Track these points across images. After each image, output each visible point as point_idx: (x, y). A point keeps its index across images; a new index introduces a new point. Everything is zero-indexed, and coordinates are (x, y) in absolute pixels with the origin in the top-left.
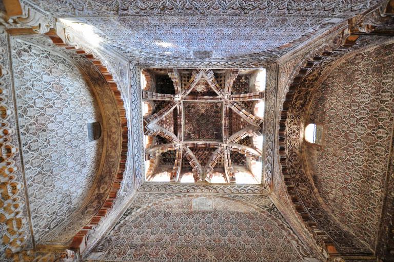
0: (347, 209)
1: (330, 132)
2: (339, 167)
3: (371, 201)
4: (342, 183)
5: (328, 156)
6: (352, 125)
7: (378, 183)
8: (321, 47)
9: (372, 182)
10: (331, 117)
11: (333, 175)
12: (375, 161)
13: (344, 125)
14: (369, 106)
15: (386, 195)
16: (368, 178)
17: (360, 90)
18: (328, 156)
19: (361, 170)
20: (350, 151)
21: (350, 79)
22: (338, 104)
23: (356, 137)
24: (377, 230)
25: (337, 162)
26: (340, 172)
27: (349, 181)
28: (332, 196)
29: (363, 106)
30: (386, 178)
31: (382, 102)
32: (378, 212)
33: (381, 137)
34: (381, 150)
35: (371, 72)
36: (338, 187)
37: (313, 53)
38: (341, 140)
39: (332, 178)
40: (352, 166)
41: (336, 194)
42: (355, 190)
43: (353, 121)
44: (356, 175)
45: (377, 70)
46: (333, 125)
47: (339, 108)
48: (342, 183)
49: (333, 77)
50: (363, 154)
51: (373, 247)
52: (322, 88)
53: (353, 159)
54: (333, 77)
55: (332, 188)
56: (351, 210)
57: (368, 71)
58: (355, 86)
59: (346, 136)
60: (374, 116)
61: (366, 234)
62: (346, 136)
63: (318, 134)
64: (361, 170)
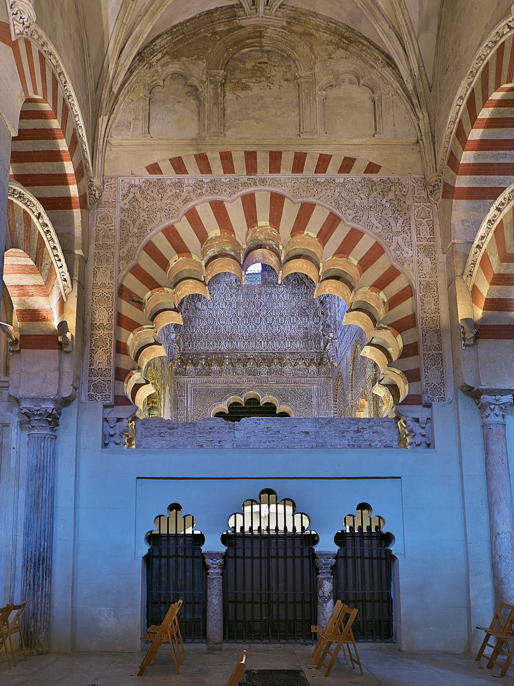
0: (197, 323)
1: (257, 296)
5: (234, 296)
6: (266, 318)
8: (328, 311)
10: (270, 294)
11: (219, 304)
13: (265, 311)
14: (282, 332)
15: (225, 353)
16: (231, 338)
17: (294, 323)
18: (234, 296)
19: (234, 332)
20: (246, 321)
21: (303, 313)
22: (282, 302)
23: (258, 324)
26: (225, 312)
29: (282, 327)
31: (284, 342)
32: (211, 350)
33: (261, 344)
34: (252, 345)
35: (306, 331)
37: (326, 301)
38: (253, 310)
42: (217, 329)
43: (269, 320)
45: (306, 336)
46: (264, 299)
47: (279, 304)
49: (307, 293)
50: (246, 332)
52: (298, 281)
53: (240, 324)
54: (307, 293)
56: (199, 327)
57: (306, 328)
58: (297, 319)
59: (257, 315)
60: (275, 337)
61: (189, 342)
62: (257, 315)
64: (234, 332)
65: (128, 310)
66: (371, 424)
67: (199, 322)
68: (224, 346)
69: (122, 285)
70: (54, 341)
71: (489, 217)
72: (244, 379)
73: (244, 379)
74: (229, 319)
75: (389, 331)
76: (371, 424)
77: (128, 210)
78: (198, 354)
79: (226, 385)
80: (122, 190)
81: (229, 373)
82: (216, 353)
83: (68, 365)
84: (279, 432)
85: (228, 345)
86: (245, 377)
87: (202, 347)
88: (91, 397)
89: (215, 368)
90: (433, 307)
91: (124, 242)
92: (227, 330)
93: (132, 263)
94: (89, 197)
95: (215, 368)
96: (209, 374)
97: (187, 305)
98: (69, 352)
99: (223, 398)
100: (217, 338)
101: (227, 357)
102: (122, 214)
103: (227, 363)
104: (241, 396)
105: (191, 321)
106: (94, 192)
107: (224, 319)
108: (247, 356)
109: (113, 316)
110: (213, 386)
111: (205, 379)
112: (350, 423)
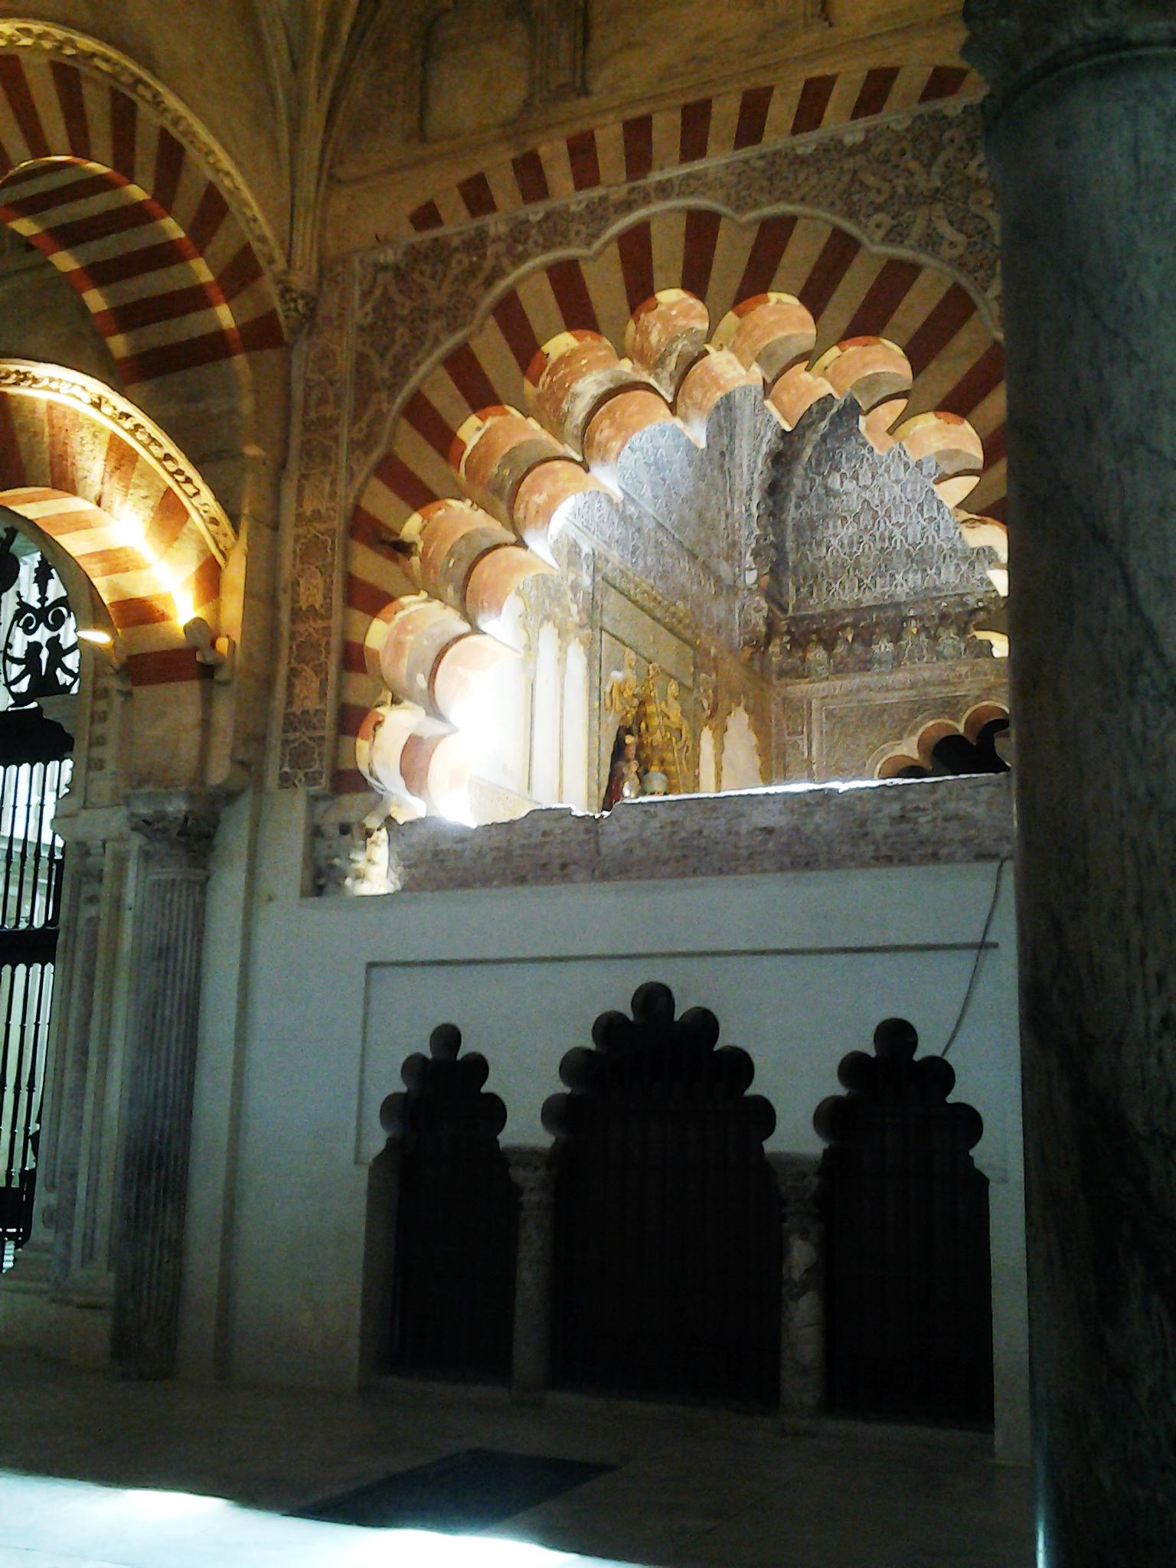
0: (831, 531)
2: (915, 482)
3: (878, 580)
4: (882, 502)
7: (919, 582)
9: (916, 572)
11: (887, 470)
12: (957, 565)
15: (905, 603)
24: (832, 606)
25: (925, 472)
27: (894, 521)
28: (834, 481)
30: (935, 594)
36: (867, 495)
39: (881, 471)
40: (932, 519)
41: (846, 493)
44: (914, 532)
48: (882, 502)
51: (797, 608)
53: (947, 516)
56: (835, 542)
61: (811, 586)
65: (369, 565)
66: (937, 796)
67: (835, 527)
68: (904, 584)
69: (357, 508)
70: (190, 663)
72: (963, 670)
73: (963, 670)
74: (914, 508)
76: (937, 796)
77: (372, 327)
78: (833, 615)
79: (913, 692)
80: (361, 283)
81: (921, 658)
82: (881, 608)
83: (224, 715)
84: (700, 832)
85: (915, 579)
86: (966, 664)
87: (846, 595)
88: (286, 780)
89: (884, 647)
91: (362, 404)
92: (910, 540)
93: (377, 454)
94: (286, 317)
95: (884, 647)
96: (865, 666)
97: (803, 486)
98: (226, 683)
99: (904, 729)
100: (885, 565)
101: (912, 613)
102: (360, 340)
103: (915, 631)
104: (955, 717)
105: (814, 529)
106: (292, 305)
107: (903, 508)
108: (966, 604)
110: (880, 699)
111: (856, 681)
112: (882, 795)
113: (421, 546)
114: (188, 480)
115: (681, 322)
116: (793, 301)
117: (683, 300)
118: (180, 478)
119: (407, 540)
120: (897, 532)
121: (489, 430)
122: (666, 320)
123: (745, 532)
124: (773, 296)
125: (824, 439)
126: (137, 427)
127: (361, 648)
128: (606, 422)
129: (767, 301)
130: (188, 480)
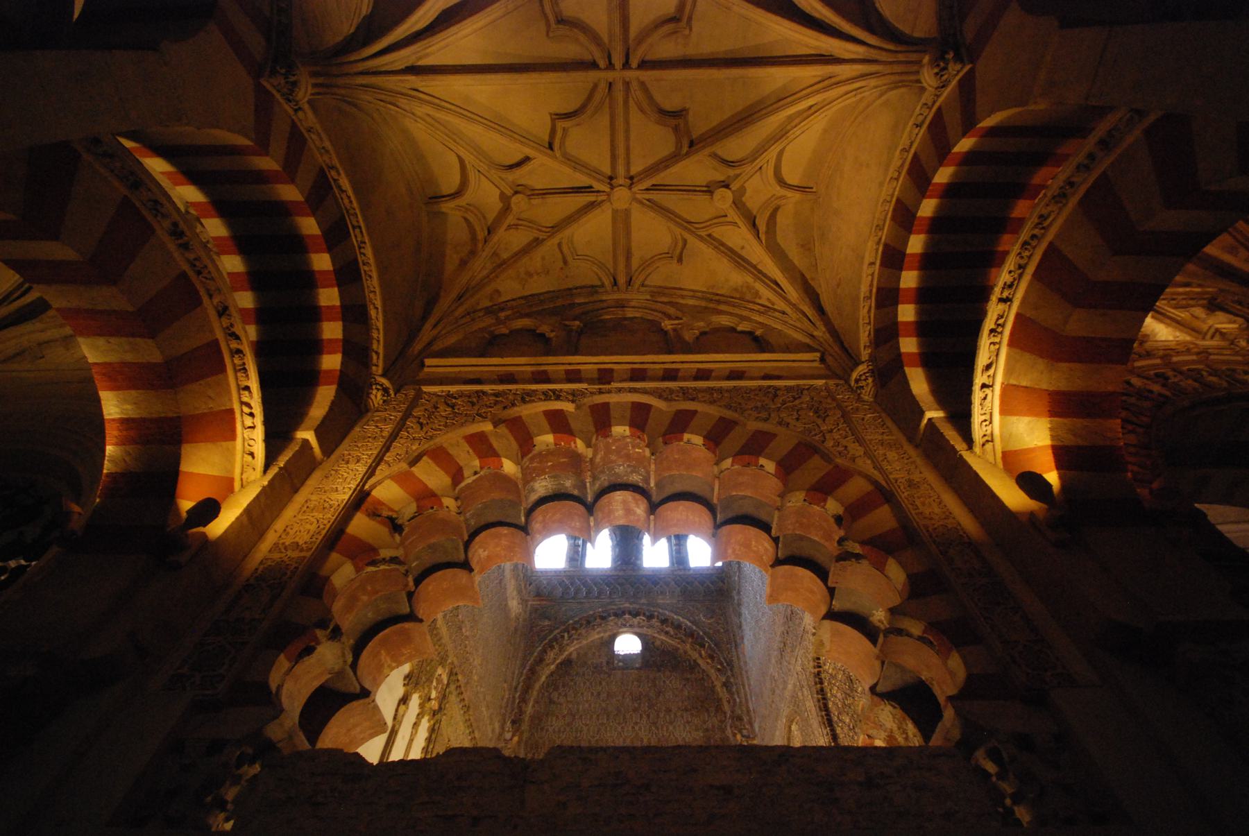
6: (648, 716)
17: (688, 722)
28: (555, 695)
29: (671, 728)
55: (566, 695)
56: (551, 729)
57: (707, 730)
63: (628, 658)
71: (989, 324)
75: (865, 563)
90: (937, 510)
109: (324, 532)
113: (406, 530)
114: (252, 415)
115: (613, 457)
116: (698, 440)
117: (624, 437)
118: (246, 410)
119: (399, 522)
120: (585, 729)
121: (481, 478)
122: (608, 451)
123: (509, 709)
124: (686, 436)
125: (552, 674)
126: (239, 352)
127: (327, 579)
128: (540, 518)
129: (681, 440)
130: (252, 415)
